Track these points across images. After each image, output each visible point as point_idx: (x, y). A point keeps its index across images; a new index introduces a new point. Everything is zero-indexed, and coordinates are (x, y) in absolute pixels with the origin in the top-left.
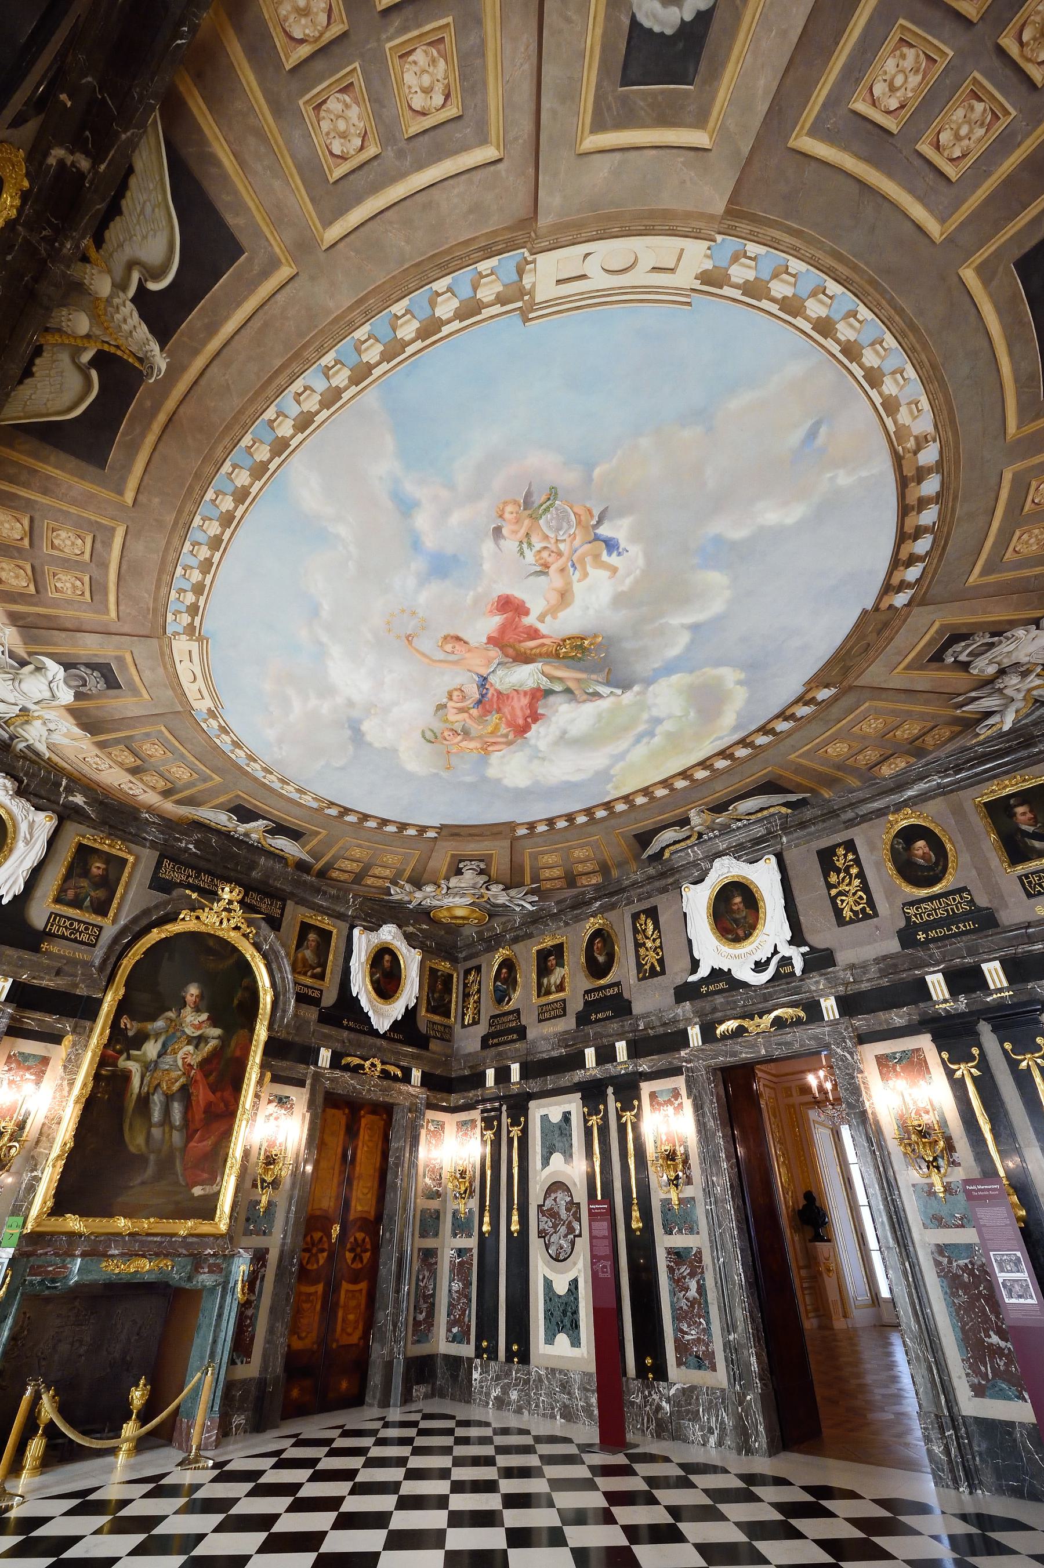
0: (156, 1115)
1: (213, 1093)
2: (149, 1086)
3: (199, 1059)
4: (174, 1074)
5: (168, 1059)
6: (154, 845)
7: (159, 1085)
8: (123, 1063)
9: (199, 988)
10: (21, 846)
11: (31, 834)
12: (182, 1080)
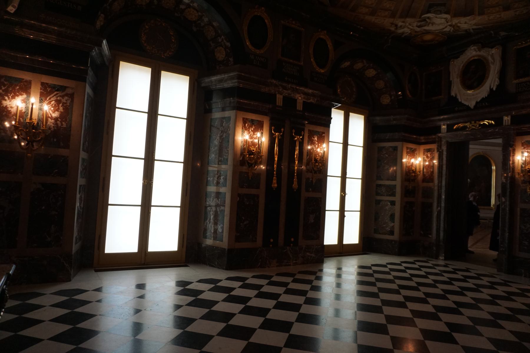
10: (492, 66)
11: (493, 59)
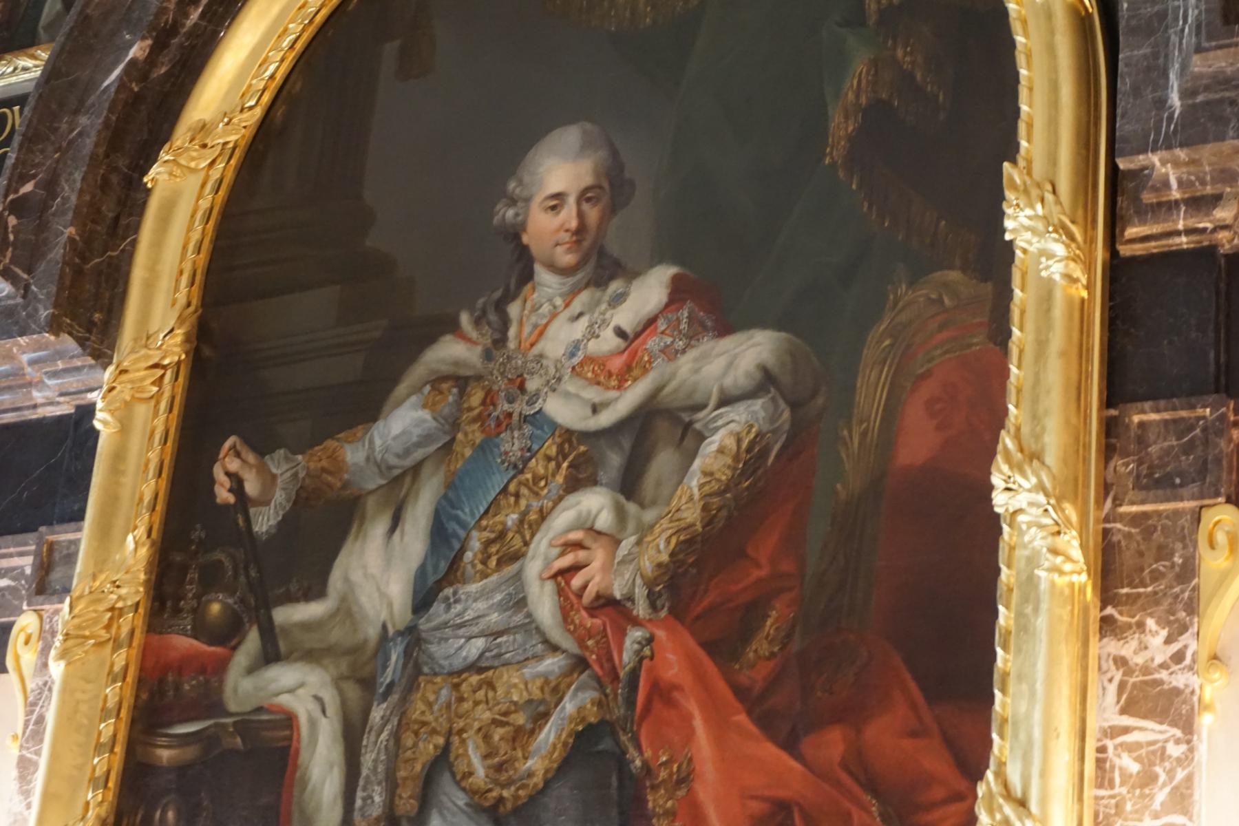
1: (790, 745)
3: (659, 549)
4: (517, 684)
5: (477, 600)
7: (442, 760)
8: (249, 685)
9: (586, 145)
12: (575, 704)
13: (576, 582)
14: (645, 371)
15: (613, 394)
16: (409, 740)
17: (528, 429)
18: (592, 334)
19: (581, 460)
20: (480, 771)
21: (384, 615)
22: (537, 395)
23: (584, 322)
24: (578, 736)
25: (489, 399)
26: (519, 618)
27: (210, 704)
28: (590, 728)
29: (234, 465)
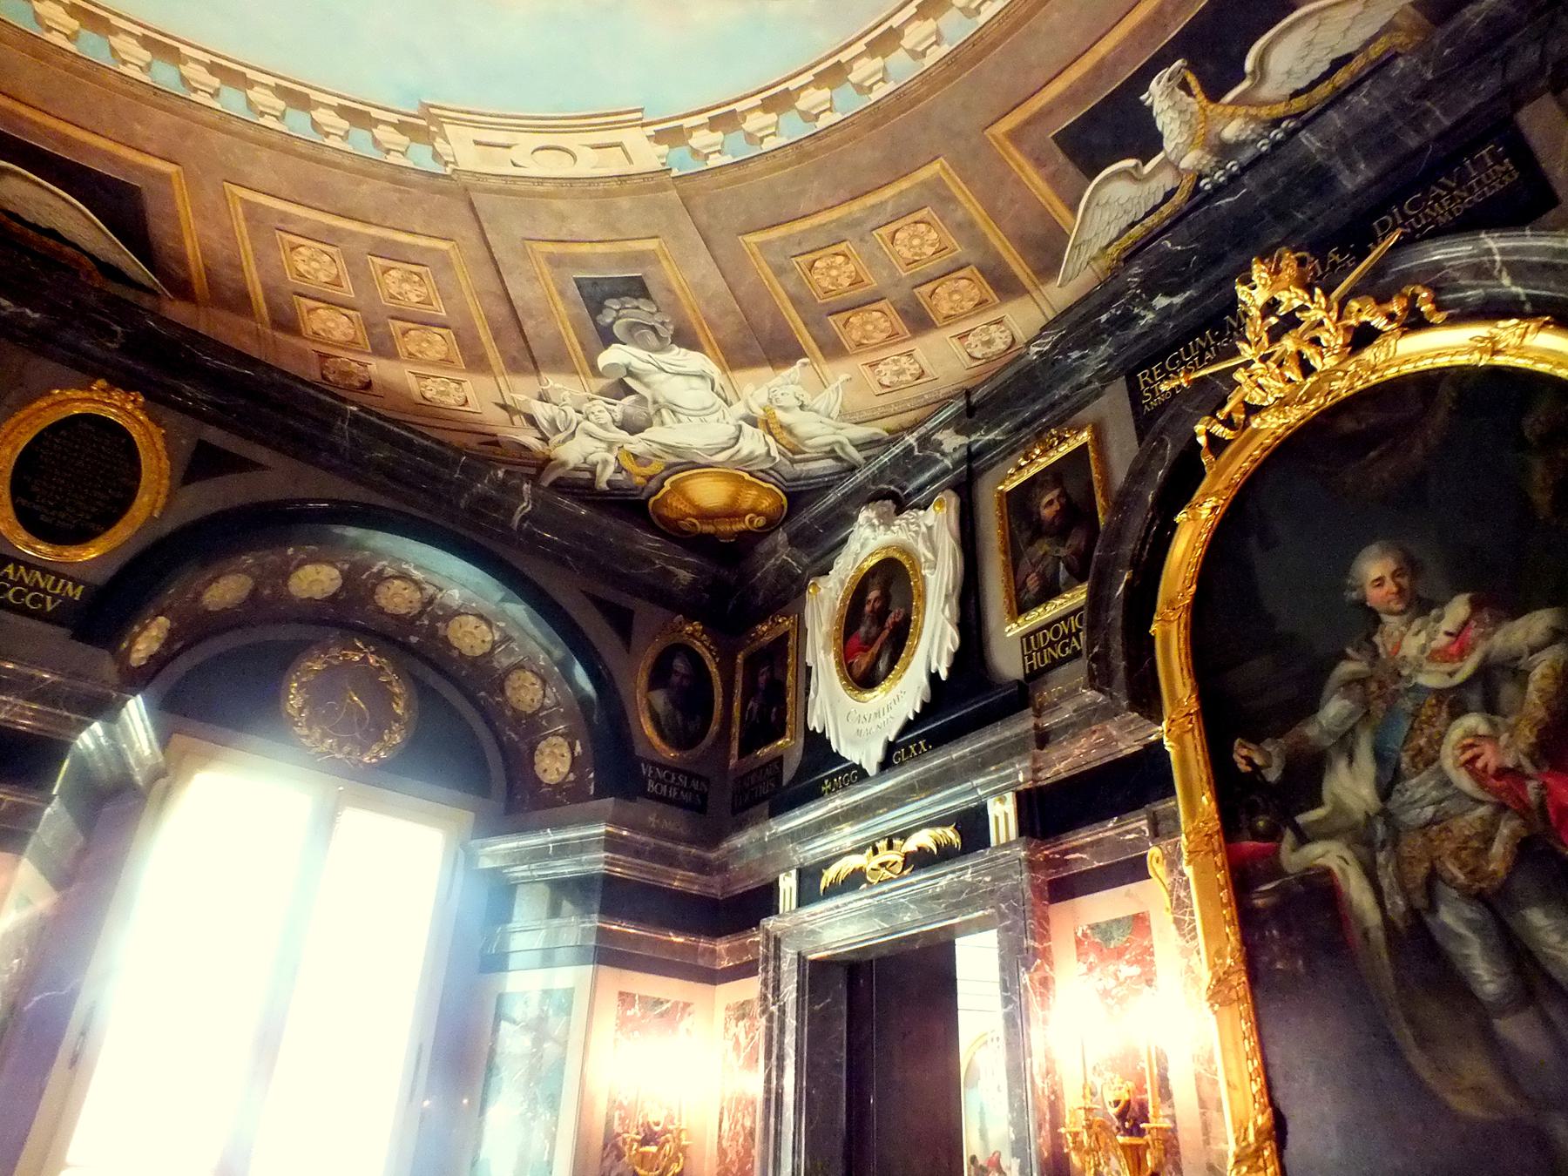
0: (1486, 975)
2: (1406, 894)
3: (1527, 736)
6: (1106, 379)
7: (1433, 877)
8: (1294, 858)
9: (1385, 552)
11: (934, 551)
12: (1506, 830)
13: (1479, 764)
14: (1473, 649)
15: (1458, 665)
16: (1406, 868)
17: (1412, 695)
18: (1431, 638)
19: (1454, 702)
20: (1461, 877)
21: (1364, 807)
22: (1410, 677)
23: (1423, 635)
24: (1519, 846)
25: (1382, 685)
26: (1449, 792)
27: (1276, 871)
28: (1524, 840)
29: (1244, 752)
